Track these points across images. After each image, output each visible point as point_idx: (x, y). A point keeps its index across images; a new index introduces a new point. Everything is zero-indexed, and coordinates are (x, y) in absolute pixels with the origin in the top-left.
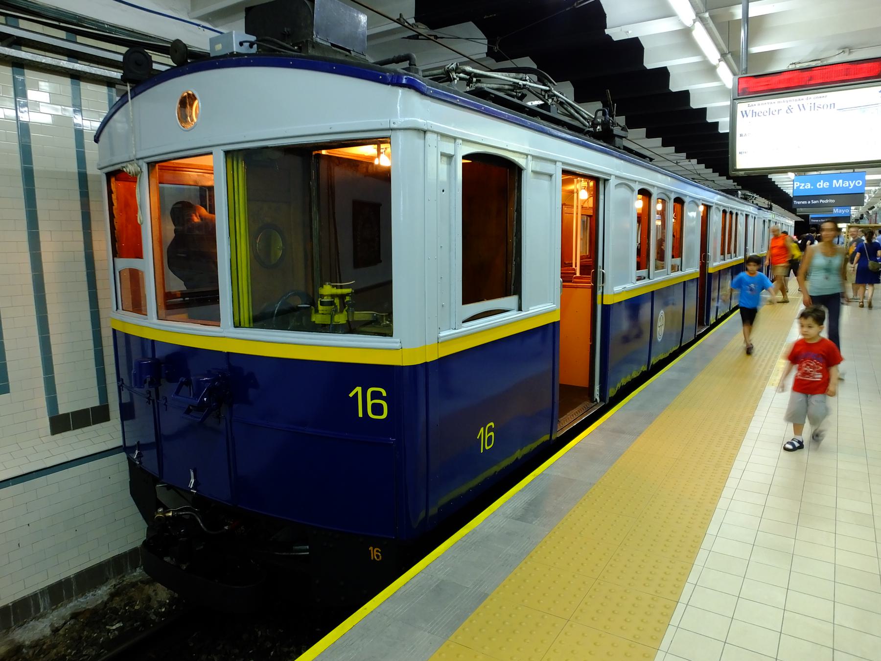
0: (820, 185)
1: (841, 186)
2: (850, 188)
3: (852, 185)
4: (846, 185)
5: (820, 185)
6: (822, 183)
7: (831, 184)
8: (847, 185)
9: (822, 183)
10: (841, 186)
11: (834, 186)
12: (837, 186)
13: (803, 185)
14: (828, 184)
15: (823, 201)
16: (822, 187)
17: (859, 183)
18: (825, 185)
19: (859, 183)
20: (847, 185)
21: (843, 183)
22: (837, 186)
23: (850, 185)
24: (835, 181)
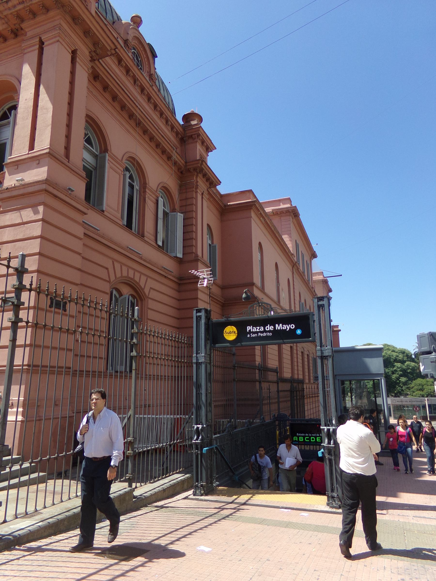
0: (267, 328)
1: (281, 329)
2: (287, 330)
3: (288, 328)
5: (267, 328)
6: (268, 327)
7: (275, 327)
8: (285, 328)
9: (268, 327)
10: (281, 329)
11: (277, 329)
12: (279, 329)
13: (259, 328)
14: (273, 327)
15: (262, 335)
16: (269, 329)
17: (292, 326)
19: (292, 326)
20: (285, 328)
21: (282, 327)
22: (279, 329)
23: (287, 329)
24: (277, 325)
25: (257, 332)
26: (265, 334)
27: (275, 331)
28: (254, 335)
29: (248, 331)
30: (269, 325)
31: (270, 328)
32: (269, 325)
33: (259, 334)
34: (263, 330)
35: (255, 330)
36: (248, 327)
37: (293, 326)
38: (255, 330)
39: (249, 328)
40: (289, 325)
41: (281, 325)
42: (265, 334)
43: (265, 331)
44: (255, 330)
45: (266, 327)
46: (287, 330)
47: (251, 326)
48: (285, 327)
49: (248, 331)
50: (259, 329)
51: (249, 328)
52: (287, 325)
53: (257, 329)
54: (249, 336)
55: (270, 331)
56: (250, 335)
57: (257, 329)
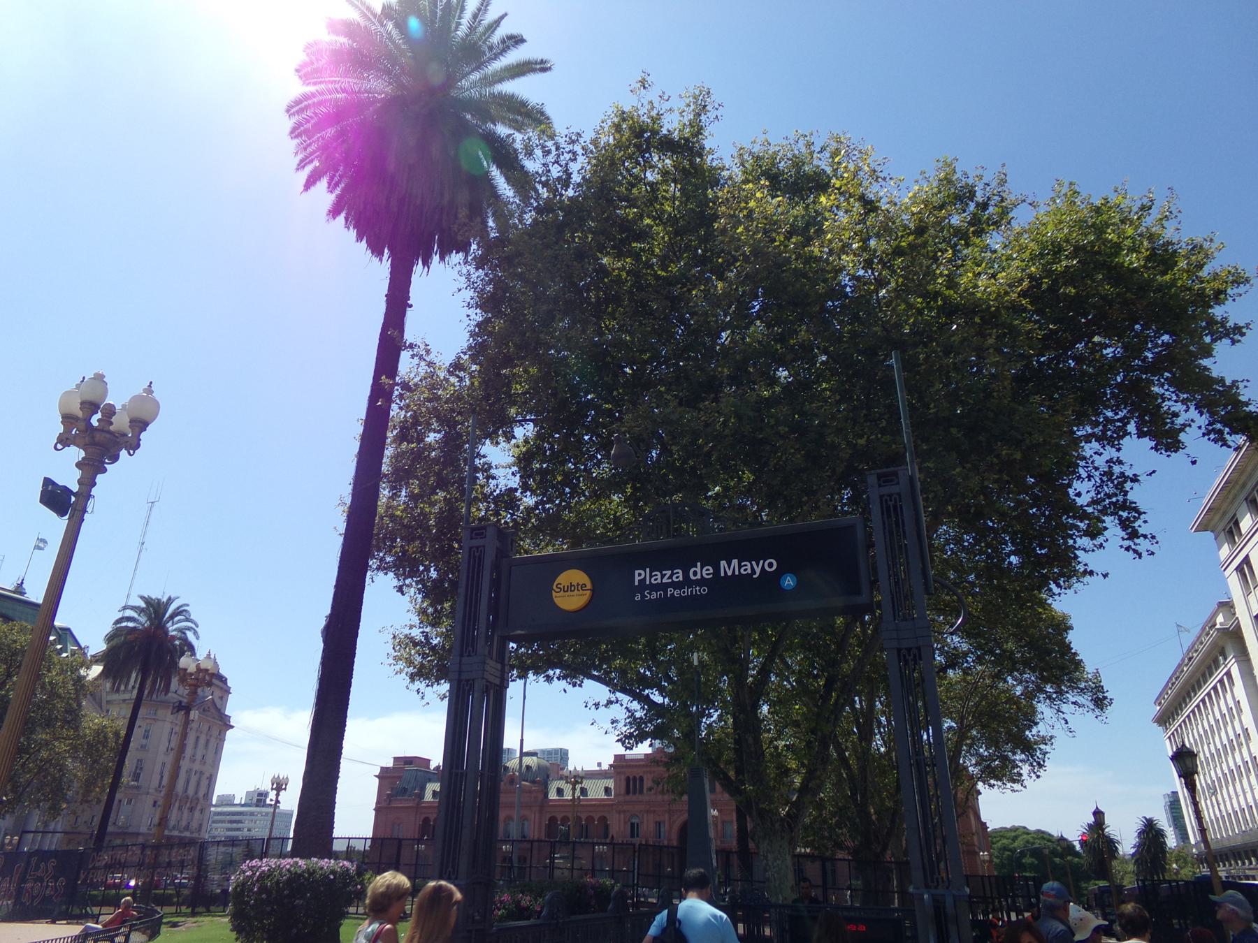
0: (695, 573)
1: (737, 573)
2: (754, 576)
3: (758, 570)
4: (745, 570)
5: (695, 573)
9: (698, 570)
10: (737, 573)
11: (722, 574)
12: (730, 573)
13: (669, 573)
14: (711, 571)
16: (699, 576)
17: (771, 565)
18: (704, 572)
19: (771, 565)
20: (749, 571)
21: (740, 567)
22: (730, 573)
24: (723, 563)
25: (663, 587)
26: (686, 591)
27: (717, 582)
28: (654, 596)
29: (637, 584)
30: (699, 564)
31: (701, 571)
32: (699, 564)
33: (670, 591)
34: (681, 579)
35: (659, 581)
36: (637, 572)
37: (771, 565)
38: (657, 578)
39: (639, 575)
40: (761, 562)
41: (735, 562)
42: (686, 591)
43: (687, 582)
44: (657, 578)
45: (692, 570)
46: (754, 576)
47: (648, 570)
48: (749, 567)
49: (637, 584)
50: (670, 577)
51: (640, 575)
52: (754, 563)
53: (663, 576)
54: (638, 597)
55: (702, 582)
56: (643, 596)
57: (663, 576)
